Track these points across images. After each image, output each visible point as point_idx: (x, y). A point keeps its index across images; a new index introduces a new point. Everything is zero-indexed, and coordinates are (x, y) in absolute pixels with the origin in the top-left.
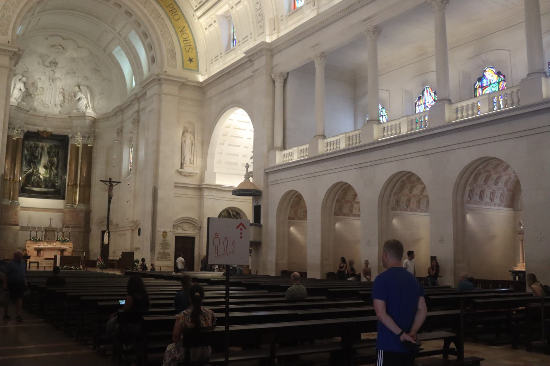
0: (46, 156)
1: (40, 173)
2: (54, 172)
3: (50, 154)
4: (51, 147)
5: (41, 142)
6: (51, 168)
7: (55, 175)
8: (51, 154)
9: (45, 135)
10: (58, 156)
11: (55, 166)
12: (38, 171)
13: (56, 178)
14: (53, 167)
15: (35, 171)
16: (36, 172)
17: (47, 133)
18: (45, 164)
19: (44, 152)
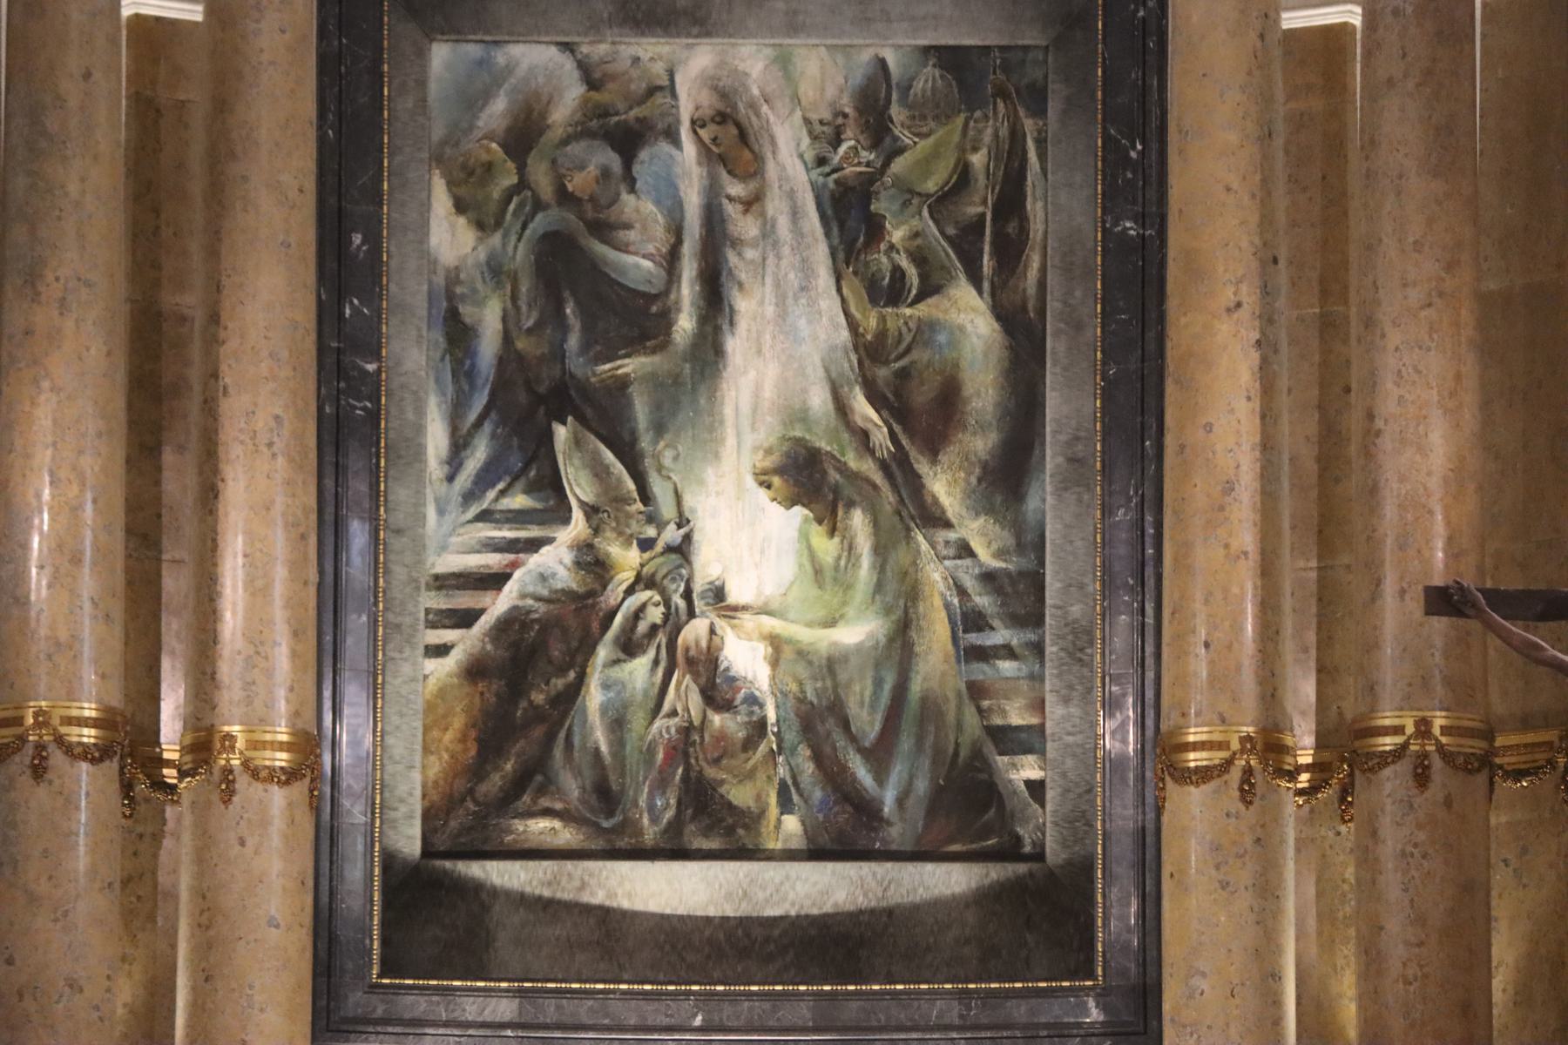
0: (806, 269)
1: (718, 594)
2: (965, 550)
3: (875, 228)
6: (901, 472)
7: (983, 601)
8: (897, 235)
10: (1010, 252)
11: (981, 443)
12: (682, 550)
13: (1009, 652)
14: (933, 451)
15: (626, 559)
16: (643, 581)
19: (752, 203)
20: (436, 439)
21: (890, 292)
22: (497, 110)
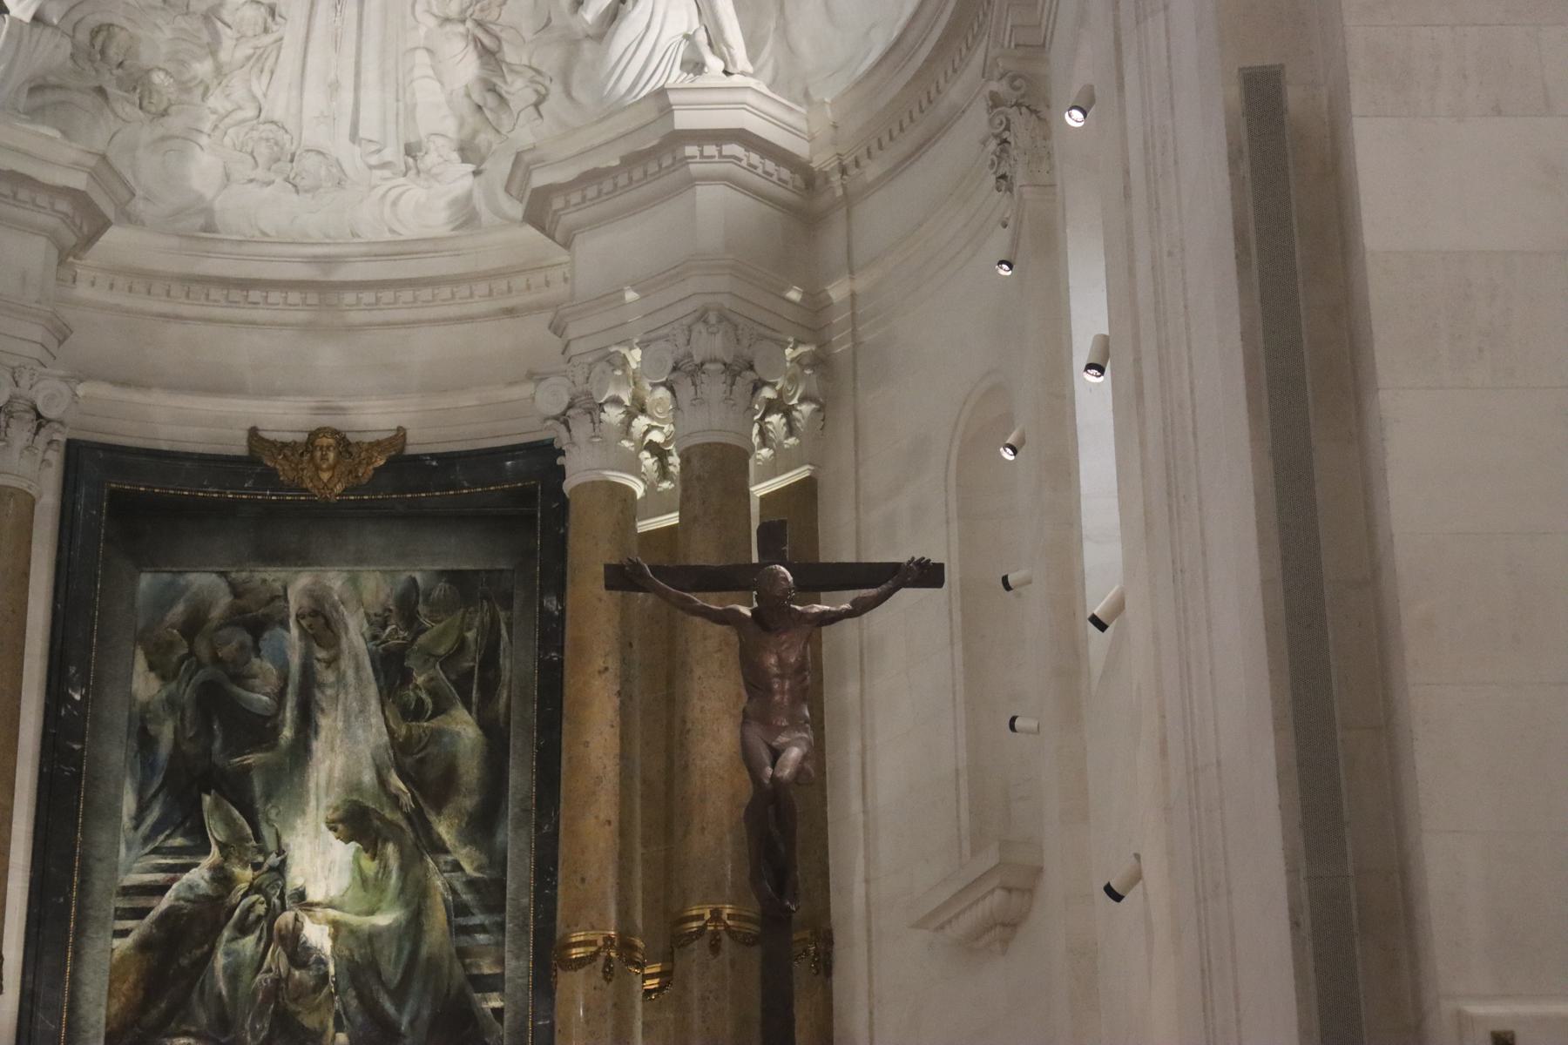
0: (364, 702)
1: (300, 895)
2: (457, 867)
3: (407, 677)
4: (407, 605)
5: (301, 558)
7: (467, 897)
8: (420, 680)
9: (329, 482)
10: (489, 688)
11: (469, 803)
12: (280, 870)
13: (482, 929)
14: (439, 809)
15: (245, 875)
16: (254, 888)
17: (343, 443)
18: (354, 787)
19: (332, 662)
20: (129, 804)
21: (414, 713)
22: (179, 610)
